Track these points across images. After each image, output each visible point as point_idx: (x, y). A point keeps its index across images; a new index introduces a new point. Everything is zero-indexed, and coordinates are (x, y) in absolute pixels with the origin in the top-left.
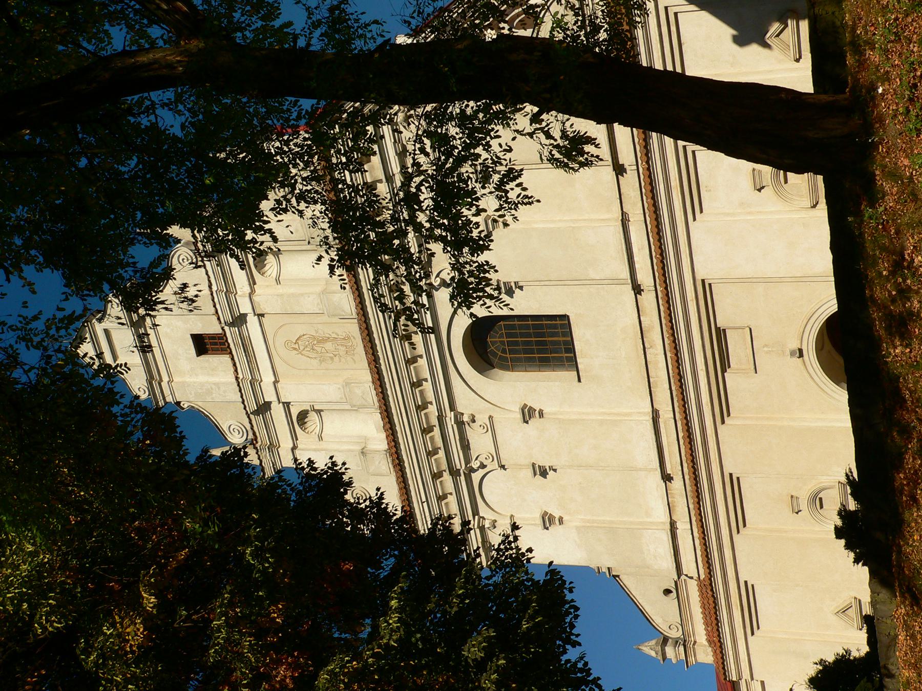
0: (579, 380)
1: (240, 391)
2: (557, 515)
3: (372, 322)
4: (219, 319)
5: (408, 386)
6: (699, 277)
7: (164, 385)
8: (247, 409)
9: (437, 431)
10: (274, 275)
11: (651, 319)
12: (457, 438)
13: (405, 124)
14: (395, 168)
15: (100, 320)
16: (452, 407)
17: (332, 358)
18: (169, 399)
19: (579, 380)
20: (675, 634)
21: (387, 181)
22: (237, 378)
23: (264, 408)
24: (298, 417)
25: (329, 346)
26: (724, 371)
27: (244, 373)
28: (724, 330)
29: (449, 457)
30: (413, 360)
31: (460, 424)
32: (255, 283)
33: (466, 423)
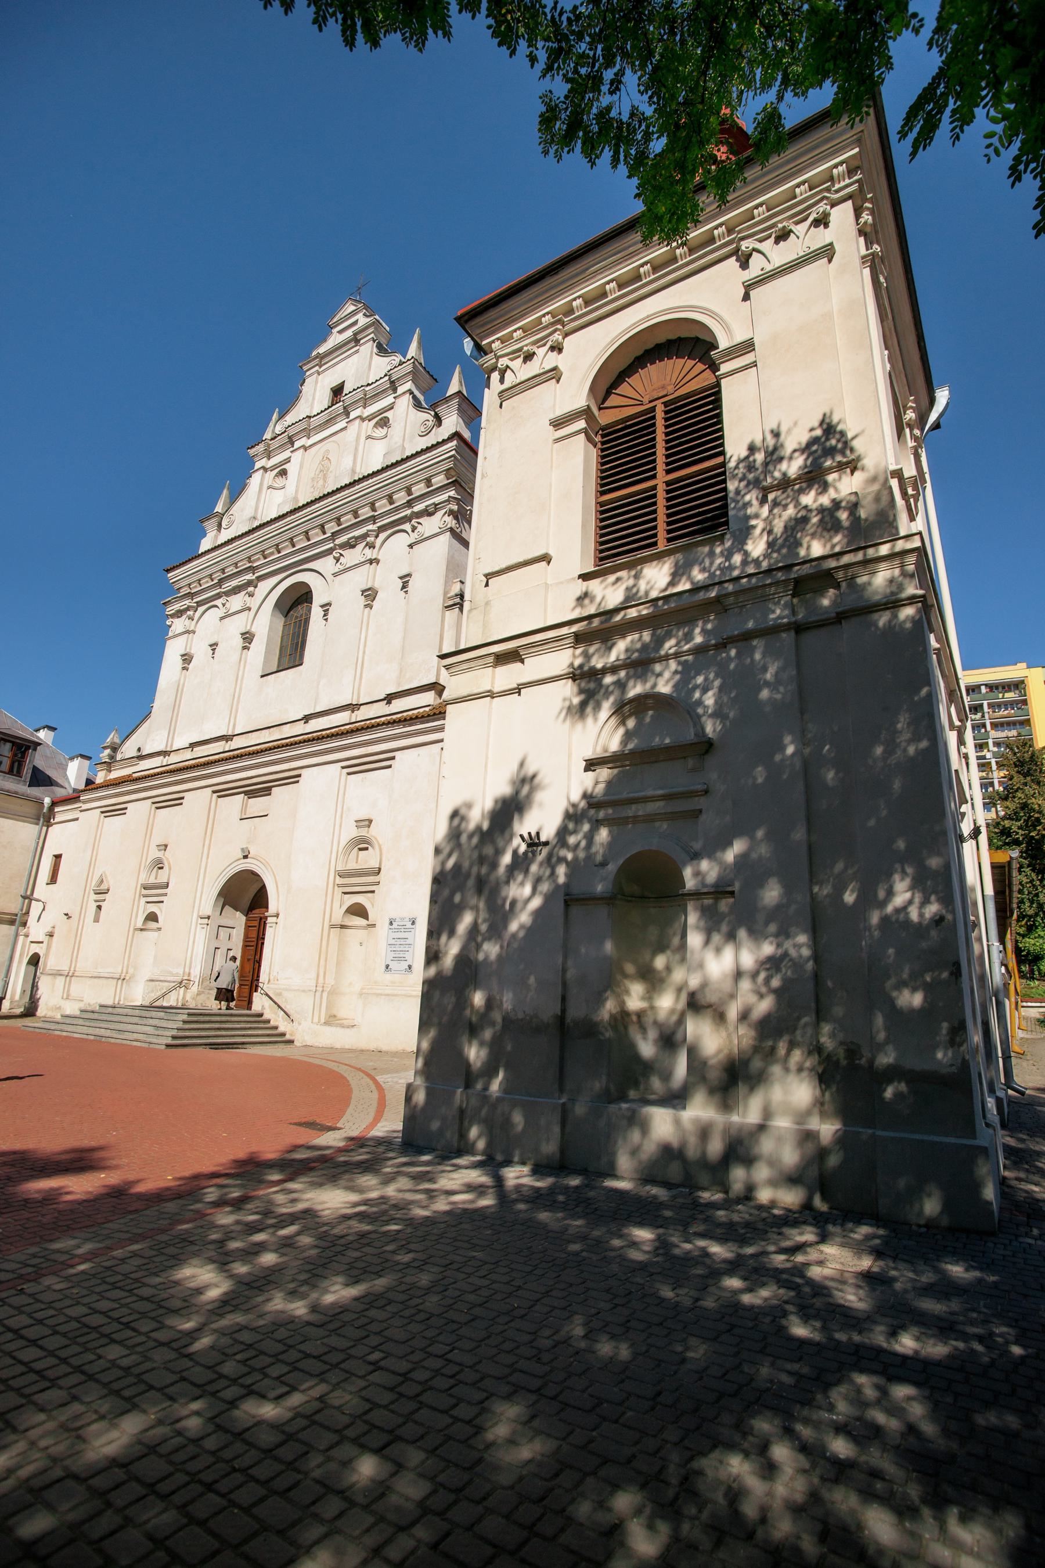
0: (262, 676)
2: (191, 666)
3: (317, 505)
6: (303, 772)
7: (317, 368)
10: (374, 435)
11: (288, 731)
15: (364, 315)
16: (260, 579)
18: (308, 373)
19: (262, 676)
20: (119, 757)
22: (309, 417)
23: (291, 441)
25: (321, 482)
26: (246, 793)
27: (315, 422)
28: (270, 794)
31: (249, 583)
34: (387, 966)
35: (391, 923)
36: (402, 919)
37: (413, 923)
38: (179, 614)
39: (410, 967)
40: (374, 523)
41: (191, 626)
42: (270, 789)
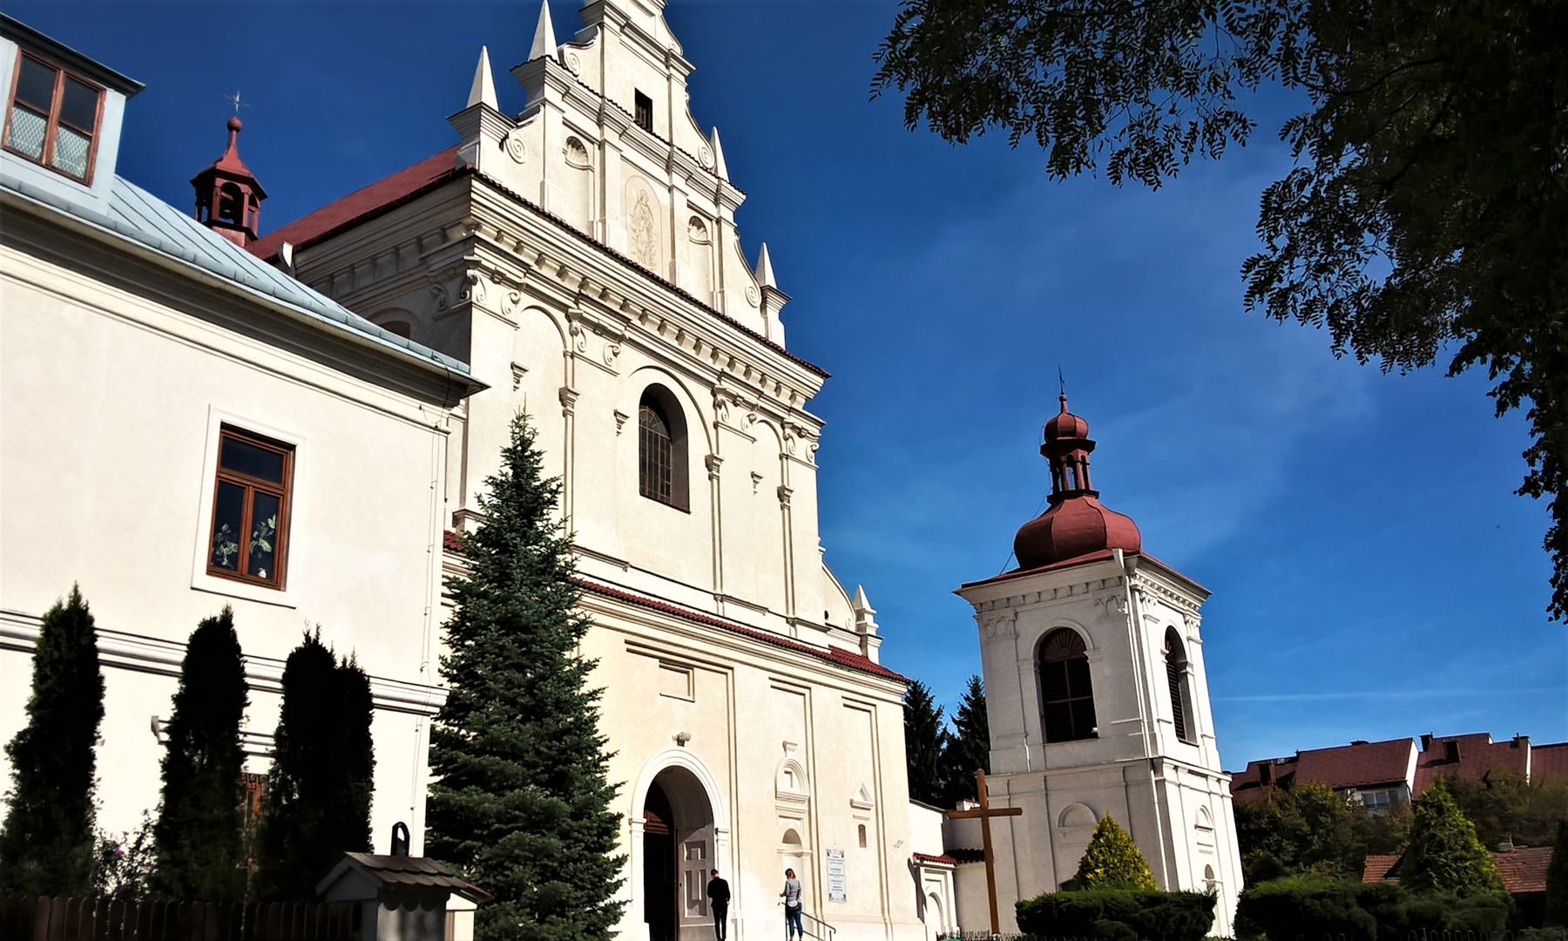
1: (626, 112)
4: (681, 150)
5: (647, 306)
8: (610, 103)
9: (616, 308)
12: (610, 328)
13: (814, 448)
14: (800, 423)
17: (635, 231)
21: (791, 408)
24: (580, 142)
26: (661, 660)
29: (595, 304)
30: (661, 328)
31: (620, 338)
32: (688, 206)
33: (617, 345)
34: (830, 895)
35: (828, 855)
36: (835, 851)
37: (843, 856)
38: (497, 277)
39: (845, 896)
40: (758, 399)
41: (516, 314)
42: (691, 667)
